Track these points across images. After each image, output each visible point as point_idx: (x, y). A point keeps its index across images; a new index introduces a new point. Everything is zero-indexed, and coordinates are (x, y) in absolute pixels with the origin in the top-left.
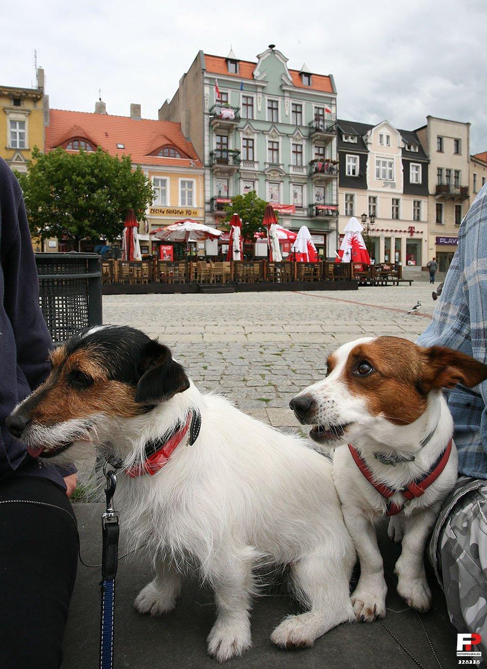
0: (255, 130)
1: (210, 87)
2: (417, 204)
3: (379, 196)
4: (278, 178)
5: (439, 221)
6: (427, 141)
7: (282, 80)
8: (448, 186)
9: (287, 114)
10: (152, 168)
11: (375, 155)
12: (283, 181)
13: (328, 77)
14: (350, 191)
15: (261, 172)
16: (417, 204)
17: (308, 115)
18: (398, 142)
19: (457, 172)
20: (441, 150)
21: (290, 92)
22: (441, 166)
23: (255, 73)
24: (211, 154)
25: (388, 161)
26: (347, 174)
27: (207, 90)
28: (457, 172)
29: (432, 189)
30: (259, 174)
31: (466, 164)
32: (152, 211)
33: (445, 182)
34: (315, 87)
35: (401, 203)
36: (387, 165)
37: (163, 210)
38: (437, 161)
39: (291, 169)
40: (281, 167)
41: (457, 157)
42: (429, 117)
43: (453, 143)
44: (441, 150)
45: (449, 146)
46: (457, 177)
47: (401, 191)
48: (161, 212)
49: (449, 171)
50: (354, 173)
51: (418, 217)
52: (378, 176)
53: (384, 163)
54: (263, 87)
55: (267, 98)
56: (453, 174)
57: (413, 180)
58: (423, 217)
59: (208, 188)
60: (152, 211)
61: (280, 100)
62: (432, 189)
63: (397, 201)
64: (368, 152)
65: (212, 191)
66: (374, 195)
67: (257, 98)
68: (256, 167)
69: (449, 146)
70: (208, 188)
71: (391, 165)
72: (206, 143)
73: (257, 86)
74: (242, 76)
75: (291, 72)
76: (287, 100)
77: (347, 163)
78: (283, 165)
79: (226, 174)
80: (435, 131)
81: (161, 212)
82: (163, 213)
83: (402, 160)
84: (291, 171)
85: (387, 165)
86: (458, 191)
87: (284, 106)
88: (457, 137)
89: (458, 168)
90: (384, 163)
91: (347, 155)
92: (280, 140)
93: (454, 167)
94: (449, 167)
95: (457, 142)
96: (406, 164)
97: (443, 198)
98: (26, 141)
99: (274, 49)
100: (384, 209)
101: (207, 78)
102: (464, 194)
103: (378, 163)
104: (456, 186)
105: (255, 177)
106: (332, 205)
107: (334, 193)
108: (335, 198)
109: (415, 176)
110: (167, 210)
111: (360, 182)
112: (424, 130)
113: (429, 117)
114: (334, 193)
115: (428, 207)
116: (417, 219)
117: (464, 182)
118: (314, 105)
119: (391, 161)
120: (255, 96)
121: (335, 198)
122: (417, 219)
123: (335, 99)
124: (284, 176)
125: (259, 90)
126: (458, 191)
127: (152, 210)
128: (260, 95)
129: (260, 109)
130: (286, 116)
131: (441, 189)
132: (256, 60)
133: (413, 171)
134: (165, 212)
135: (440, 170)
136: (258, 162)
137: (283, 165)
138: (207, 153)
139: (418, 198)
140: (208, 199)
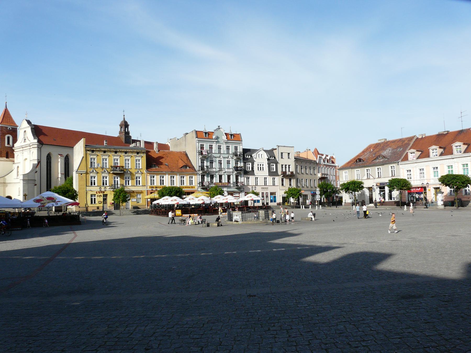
0: (214, 157)
5: (283, 185)
11: (257, 162)
13: (239, 134)
17: (232, 150)
18: (265, 156)
20: (282, 158)
24: (199, 166)
26: (247, 170)
28: (289, 166)
29: (280, 172)
36: (262, 165)
38: (281, 162)
39: (227, 169)
41: (289, 160)
46: (289, 168)
47: (268, 175)
50: (249, 169)
51: (275, 185)
52: (258, 169)
53: (260, 165)
54: (216, 141)
55: (217, 145)
59: (198, 179)
61: (222, 145)
62: (280, 172)
63: (266, 178)
64: (255, 161)
66: (256, 177)
68: (214, 170)
69: (285, 156)
71: (263, 165)
73: (214, 141)
83: (268, 163)
84: (226, 170)
85: (262, 165)
86: (290, 173)
90: (260, 165)
92: (222, 159)
95: (289, 154)
96: (269, 164)
98: (140, 166)
99: (220, 127)
100: (261, 182)
103: (258, 165)
111: (252, 173)
115: (278, 180)
119: (263, 163)
123: (242, 143)
126: (290, 173)
132: (213, 131)
135: (282, 165)
140: (198, 182)
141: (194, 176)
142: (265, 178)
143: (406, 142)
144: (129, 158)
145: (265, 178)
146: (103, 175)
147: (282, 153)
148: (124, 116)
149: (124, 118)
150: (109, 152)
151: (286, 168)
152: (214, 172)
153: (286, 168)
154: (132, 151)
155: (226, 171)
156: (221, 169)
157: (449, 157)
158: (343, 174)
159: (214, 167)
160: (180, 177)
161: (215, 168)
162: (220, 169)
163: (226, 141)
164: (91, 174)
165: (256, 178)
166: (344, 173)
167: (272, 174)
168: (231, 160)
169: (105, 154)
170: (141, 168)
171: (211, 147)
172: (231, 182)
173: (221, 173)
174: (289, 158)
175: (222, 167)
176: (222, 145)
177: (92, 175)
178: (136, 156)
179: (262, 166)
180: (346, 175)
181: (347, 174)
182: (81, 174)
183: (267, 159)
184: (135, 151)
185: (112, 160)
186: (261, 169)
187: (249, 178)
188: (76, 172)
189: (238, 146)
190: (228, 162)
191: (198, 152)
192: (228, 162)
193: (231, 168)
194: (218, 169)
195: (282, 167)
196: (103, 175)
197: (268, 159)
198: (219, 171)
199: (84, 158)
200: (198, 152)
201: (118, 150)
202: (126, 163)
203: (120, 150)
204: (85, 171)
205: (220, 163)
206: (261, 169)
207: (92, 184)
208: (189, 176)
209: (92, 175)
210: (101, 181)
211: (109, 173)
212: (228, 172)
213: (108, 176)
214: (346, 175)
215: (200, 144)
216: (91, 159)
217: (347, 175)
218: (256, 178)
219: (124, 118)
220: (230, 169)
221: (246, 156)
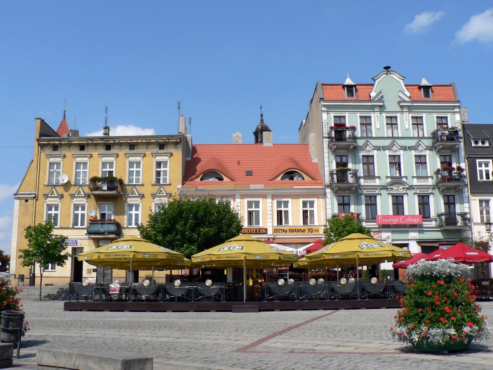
1: (327, 113)
4: (401, 190)
7: (399, 96)
9: (407, 127)
10: (274, 191)
12: (407, 194)
15: (382, 186)
21: (409, 107)
23: (371, 95)
24: (331, 174)
26: (479, 179)
27: (325, 116)
30: (380, 189)
32: (276, 231)
34: (437, 99)
37: (286, 230)
40: (404, 179)
48: (283, 231)
54: (380, 106)
55: (384, 115)
59: (329, 206)
60: (276, 231)
61: (398, 115)
65: (332, 208)
67: (374, 116)
68: (377, 182)
70: (329, 206)
72: (326, 164)
73: (373, 106)
74: (360, 99)
75: (408, 87)
76: (406, 114)
77: (478, 169)
78: (406, 177)
79: (347, 192)
81: (283, 231)
82: (286, 232)
84: (415, 182)
87: (402, 122)
91: (477, 161)
101: (324, 106)
105: (377, 192)
110: (290, 230)
118: (435, 115)
120: (372, 115)
124: (407, 188)
125: (377, 109)
127: (275, 230)
128: (378, 114)
129: (378, 126)
130: (407, 130)
134: (288, 231)
136: (379, 178)
137: (406, 177)
138: (327, 174)
141: (316, 200)
144: (138, 159)
146: (76, 201)
148: (262, 116)
149: (262, 120)
150: (93, 147)
152: (376, 188)
154: (144, 141)
155: (414, 184)
156: (397, 181)
159: (376, 175)
160: (275, 202)
161: (379, 178)
162: (394, 180)
163: (410, 104)
164: (75, 199)
168: (427, 153)
169: (82, 152)
170: (168, 182)
171: (366, 122)
172: (433, 214)
173: (398, 190)
175: (403, 175)
176: (398, 115)
177: (50, 201)
178: (158, 155)
182: (27, 201)
184: (154, 141)
185: (97, 165)
187: (487, 202)
188: (15, 195)
189: (449, 115)
190: (421, 161)
191: (325, 138)
192: (421, 161)
193: (429, 175)
194: (389, 180)
196: (76, 201)
198: (392, 184)
199: (34, 164)
200: (325, 138)
201: (111, 142)
202: (131, 173)
203: (117, 142)
204: (35, 192)
205: (395, 162)
207: (76, 223)
208: (301, 200)
209: (49, 201)
210: (70, 214)
211: (88, 196)
212: (419, 187)
213: (86, 204)
215: (332, 115)
216: (51, 164)
219: (262, 120)
220: (427, 177)
221: (476, 142)
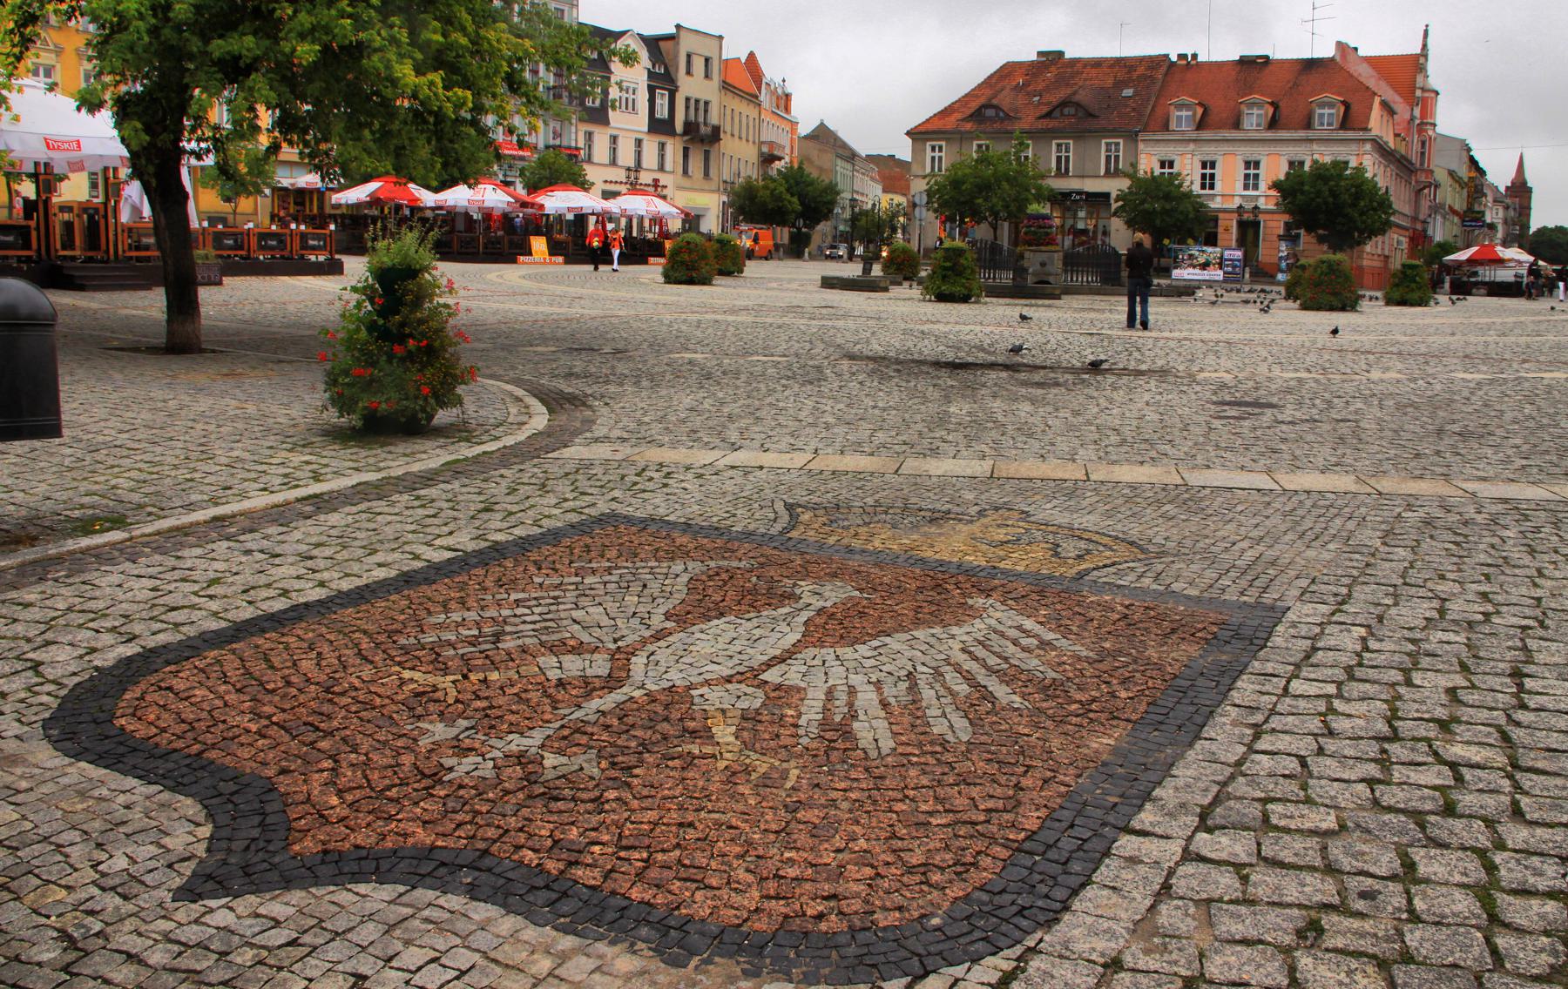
2: (662, 146)
3: (621, 134)
5: (685, 172)
6: (676, 56)
8: (697, 125)
14: (590, 128)
16: (662, 146)
19: (706, 103)
20: (689, 73)
22: (689, 95)
25: (632, 86)
28: (706, 103)
31: (717, 91)
33: (692, 117)
35: (645, 145)
36: (631, 91)
41: (707, 82)
42: (678, 27)
43: (702, 61)
44: (689, 73)
45: (698, 65)
46: (706, 111)
47: (646, 129)
49: (697, 101)
56: (692, 102)
57: (658, 116)
58: (668, 166)
64: (611, 73)
66: (615, 133)
69: (698, 65)
80: (685, 45)
86: (709, 129)
88: (708, 54)
89: (708, 98)
93: (703, 97)
94: (698, 97)
95: (707, 60)
97: (692, 140)
100: (626, 157)
102: (715, 135)
104: (705, 124)
106: (569, 148)
107: (573, 129)
108: (573, 137)
109: (662, 112)
112: (670, 43)
113: (678, 27)
114: (573, 129)
115: (673, 148)
116: (661, 168)
117: (714, 119)
121: (573, 137)
122: (661, 168)
131: (690, 128)
133: (658, 101)
135: (688, 99)
139: (663, 139)
142: (639, 142)
143: (1141, 70)
145: (639, 142)
147: (689, 56)
151: (697, 109)
153: (697, 109)
157: (1301, 134)
158: (925, 150)
165: (614, 139)
166: (929, 149)
167: (660, 126)
174: (707, 76)
179: (631, 97)
180: (937, 154)
181: (943, 154)
183: (646, 72)
186: (631, 107)
195: (687, 108)
197: (651, 75)
206: (631, 107)
214: (937, 154)
217: (940, 158)
218: (614, 139)
